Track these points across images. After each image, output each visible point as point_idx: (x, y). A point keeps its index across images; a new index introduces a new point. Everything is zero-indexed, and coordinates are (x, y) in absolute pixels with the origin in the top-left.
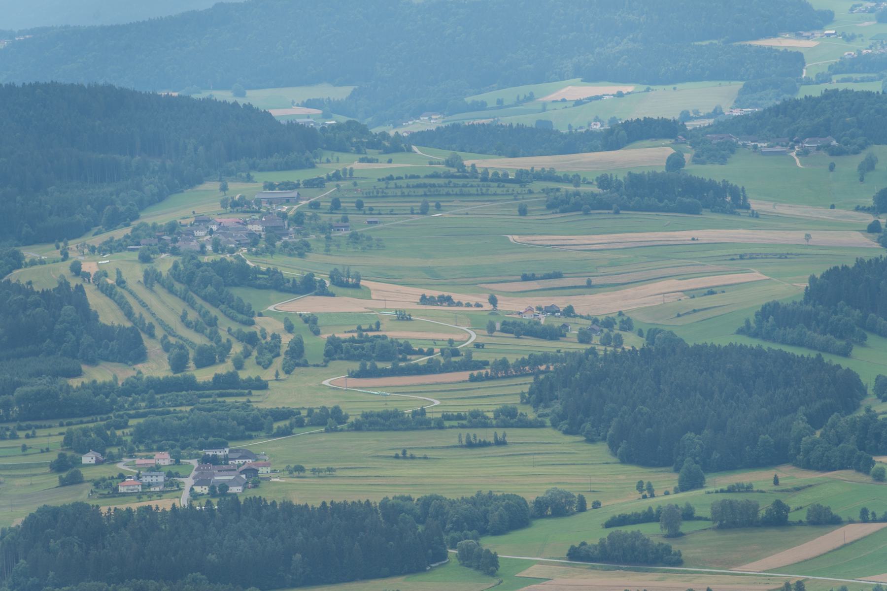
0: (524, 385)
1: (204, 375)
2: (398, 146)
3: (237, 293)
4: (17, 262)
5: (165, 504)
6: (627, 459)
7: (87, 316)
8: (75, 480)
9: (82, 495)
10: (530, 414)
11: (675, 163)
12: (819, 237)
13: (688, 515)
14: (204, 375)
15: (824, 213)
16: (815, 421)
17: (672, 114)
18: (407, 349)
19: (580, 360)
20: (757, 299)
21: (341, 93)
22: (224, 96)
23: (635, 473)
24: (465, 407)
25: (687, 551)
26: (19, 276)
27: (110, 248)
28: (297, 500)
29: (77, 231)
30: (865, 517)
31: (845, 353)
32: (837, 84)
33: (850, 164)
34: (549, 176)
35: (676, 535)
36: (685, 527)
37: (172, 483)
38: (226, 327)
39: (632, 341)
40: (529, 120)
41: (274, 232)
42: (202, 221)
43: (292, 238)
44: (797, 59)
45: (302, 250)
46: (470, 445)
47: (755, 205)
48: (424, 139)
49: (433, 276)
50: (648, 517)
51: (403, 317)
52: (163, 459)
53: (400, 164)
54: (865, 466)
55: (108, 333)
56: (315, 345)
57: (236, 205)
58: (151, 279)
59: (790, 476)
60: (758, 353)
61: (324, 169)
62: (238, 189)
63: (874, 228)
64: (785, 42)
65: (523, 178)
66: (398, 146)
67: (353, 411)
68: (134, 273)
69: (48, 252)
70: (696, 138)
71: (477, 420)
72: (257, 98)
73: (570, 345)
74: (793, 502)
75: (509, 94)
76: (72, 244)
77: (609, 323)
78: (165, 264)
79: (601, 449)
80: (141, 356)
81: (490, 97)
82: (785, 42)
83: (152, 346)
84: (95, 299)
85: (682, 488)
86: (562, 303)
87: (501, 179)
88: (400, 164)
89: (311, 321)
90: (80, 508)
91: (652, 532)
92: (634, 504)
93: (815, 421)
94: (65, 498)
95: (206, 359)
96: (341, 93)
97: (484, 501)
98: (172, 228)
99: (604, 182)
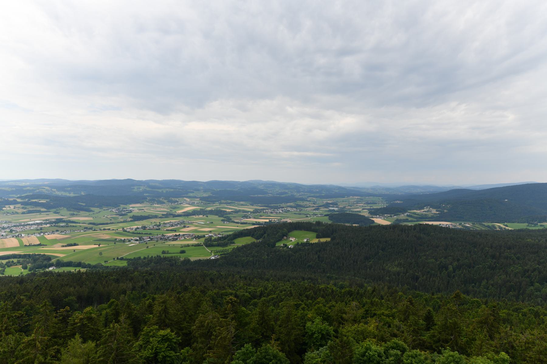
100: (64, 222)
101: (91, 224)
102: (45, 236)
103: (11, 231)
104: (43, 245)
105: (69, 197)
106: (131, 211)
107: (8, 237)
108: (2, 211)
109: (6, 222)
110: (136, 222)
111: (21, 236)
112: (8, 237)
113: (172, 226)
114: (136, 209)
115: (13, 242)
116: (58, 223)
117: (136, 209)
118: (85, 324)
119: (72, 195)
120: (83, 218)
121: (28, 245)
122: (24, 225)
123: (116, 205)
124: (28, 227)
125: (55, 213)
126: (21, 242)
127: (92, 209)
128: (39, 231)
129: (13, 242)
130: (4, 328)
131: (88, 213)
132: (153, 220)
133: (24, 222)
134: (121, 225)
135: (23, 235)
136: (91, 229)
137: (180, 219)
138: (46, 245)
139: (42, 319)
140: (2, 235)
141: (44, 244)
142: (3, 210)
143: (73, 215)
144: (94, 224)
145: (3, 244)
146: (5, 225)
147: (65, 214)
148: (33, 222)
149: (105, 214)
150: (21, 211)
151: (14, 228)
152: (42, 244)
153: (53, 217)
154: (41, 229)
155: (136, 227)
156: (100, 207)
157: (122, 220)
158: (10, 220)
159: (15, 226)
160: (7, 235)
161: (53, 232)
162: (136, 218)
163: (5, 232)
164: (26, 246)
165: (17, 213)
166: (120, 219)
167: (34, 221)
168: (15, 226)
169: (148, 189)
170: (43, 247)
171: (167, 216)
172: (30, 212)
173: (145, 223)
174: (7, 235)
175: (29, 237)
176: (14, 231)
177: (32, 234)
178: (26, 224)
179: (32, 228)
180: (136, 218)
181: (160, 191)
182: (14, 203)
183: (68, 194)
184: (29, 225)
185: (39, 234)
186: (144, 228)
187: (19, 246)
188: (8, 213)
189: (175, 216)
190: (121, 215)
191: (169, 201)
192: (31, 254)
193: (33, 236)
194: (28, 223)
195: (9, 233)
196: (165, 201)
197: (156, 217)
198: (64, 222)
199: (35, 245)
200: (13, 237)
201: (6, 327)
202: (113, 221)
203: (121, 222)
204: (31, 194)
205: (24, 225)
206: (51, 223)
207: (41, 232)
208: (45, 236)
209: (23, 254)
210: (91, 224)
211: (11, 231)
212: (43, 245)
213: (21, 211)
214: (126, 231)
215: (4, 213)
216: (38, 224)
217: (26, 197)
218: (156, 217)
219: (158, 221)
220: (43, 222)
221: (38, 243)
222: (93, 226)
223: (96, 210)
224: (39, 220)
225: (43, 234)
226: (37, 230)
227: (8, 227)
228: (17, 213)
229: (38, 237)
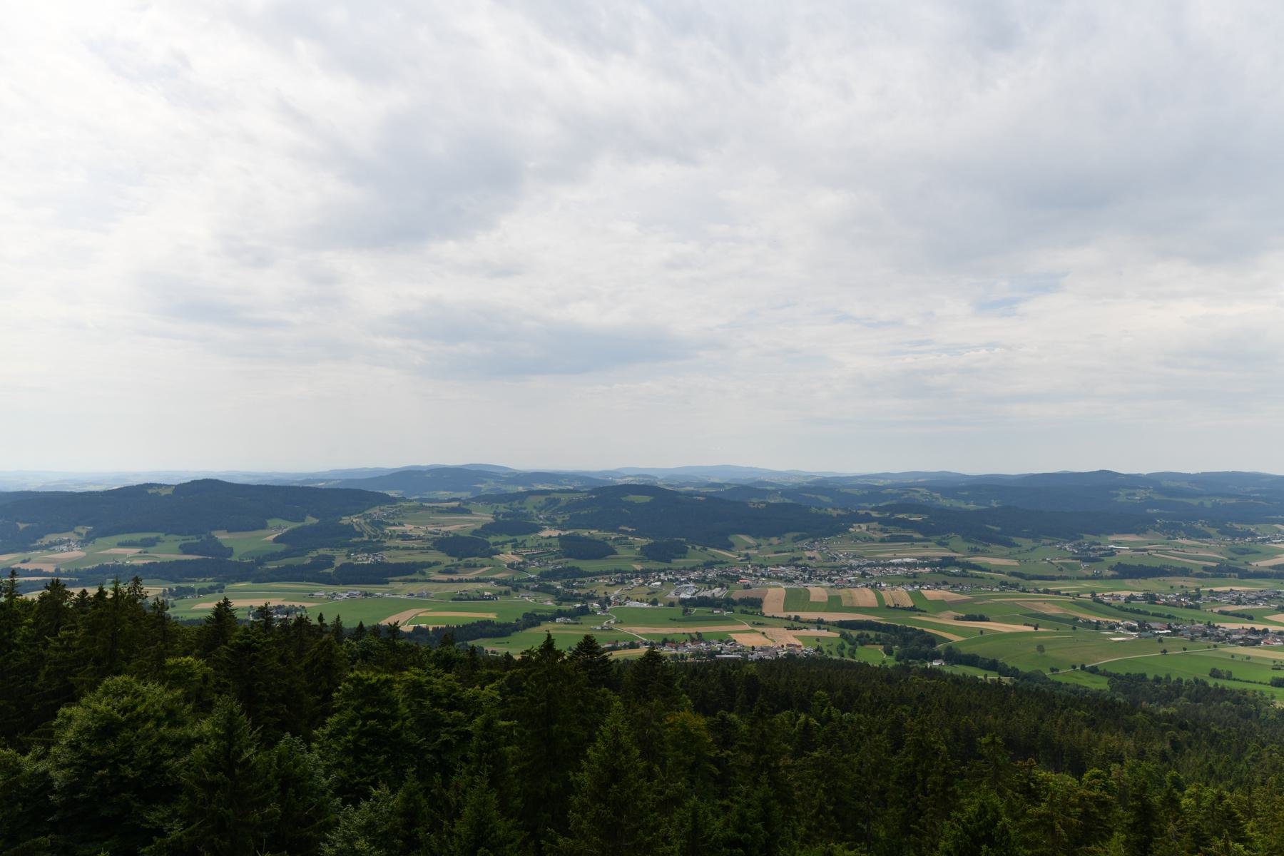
0: (431, 543)
1: (374, 540)
2: (411, 501)
3: (383, 526)
4: (341, 519)
5: (366, 562)
6: (449, 556)
7: (354, 529)
8: (350, 558)
9: (351, 561)
10: (432, 547)
11: (459, 505)
12: (484, 518)
13: (459, 565)
14: (374, 540)
15: (485, 515)
16: (482, 549)
17: (459, 497)
18: (411, 536)
19: (441, 538)
20: (474, 528)
21: (401, 492)
22: (381, 491)
23: (449, 558)
24: (422, 546)
25: (458, 571)
26: (341, 522)
27: (359, 517)
28: (390, 562)
29: (353, 515)
30: (490, 566)
31: (487, 538)
32: (488, 493)
33: (489, 506)
34: (437, 507)
35: (457, 568)
36: (459, 567)
37: (367, 559)
38: (379, 532)
39: (451, 535)
40: (434, 497)
41: (388, 515)
42: (375, 513)
43: (391, 516)
44: (480, 489)
45: (393, 519)
46: (422, 553)
47: (473, 513)
48: (415, 500)
49: (416, 524)
50: (452, 565)
51: (411, 530)
52: (366, 555)
53: (411, 504)
54: (490, 557)
55: (357, 532)
56: (395, 535)
57: (383, 511)
58: (366, 523)
59: (477, 559)
60: (473, 538)
61: (398, 505)
62: (382, 508)
63: (493, 517)
64: (478, 486)
65: (433, 507)
66: (411, 501)
67: (401, 547)
68: (363, 522)
69: (348, 518)
70: (464, 501)
71: (423, 548)
72: (386, 492)
73: (440, 536)
74: (477, 563)
75: (431, 493)
76: (352, 517)
77: (447, 532)
78: (368, 520)
79: (444, 554)
80: (363, 536)
81: (427, 493)
82: (478, 486)
83: (365, 535)
84: (355, 526)
85: (459, 560)
86: (439, 528)
87: (429, 507)
88: (411, 504)
89: (394, 531)
90: (350, 563)
91: (453, 568)
92: (449, 563)
93: (482, 549)
94: (347, 561)
95: (375, 537)
96: (401, 492)
97: (424, 562)
98: (370, 514)
99: (447, 508)
100: (957, 564)
101: (1013, 574)
102: (921, 591)
103: (864, 574)
104: (919, 610)
105: (967, 512)
106: (1112, 553)
107: (858, 586)
108: (848, 535)
109: (854, 557)
110: (1128, 582)
111: (880, 586)
112: (858, 586)
113: (1239, 602)
114: (1124, 546)
115: (866, 597)
116: (946, 566)
117: (1124, 546)
118: (1094, 813)
119: (972, 506)
120: (995, 560)
121: (893, 606)
122: (884, 566)
123: (1071, 535)
124: (891, 570)
125: (940, 544)
126: (880, 598)
127: (1016, 540)
128: (912, 581)
129: (866, 597)
130: (941, 769)
131: (1006, 550)
132: (1178, 581)
133: (884, 559)
134: (1087, 584)
135: (883, 585)
136: (1015, 586)
137: (1268, 586)
138: (925, 612)
139: (989, 772)
140: (850, 581)
141: (924, 609)
142: (850, 533)
143: (975, 551)
144: (1021, 576)
145: (852, 598)
146: (854, 562)
147: (958, 549)
148: (900, 560)
149: (1049, 555)
150: (878, 535)
151: (867, 570)
152: (917, 608)
153: (936, 553)
154: (915, 576)
155: (1128, 593)
156: (1035, 535)
157: (1089, 573)
158: (860, 551)
159: (868, 565)
160: (857, 582)
161: (937, 586)
162: (1127, 572)
163: (854, 575)
164: (888, 607)
165: (872, 540)
166: (1085, 569)
167: (902, 558)
168: (868, 565)
169: (1157, 497)
170: (919, 615)
171: (1220, 572)
172: (894, 539)
173: (1152, 585)
174: (857, 582)
175: (893, 589)
176: (868, 574)
177: (899, 586)
178: (888, 562)
179: (898, 573)
180: (1127, 572)
181: (1196, 502)
182: (867, 519)
183: (962, 505)
184: (893, 565)
185: (913, 586)
186: (1151, 599)
187: (877, 605)
188: (858, 539)
189: (1245, 575)
190: (1085, 560)
191: (1222, 533)
192: (899, 625)
193: (900, 589)
194: (890, 561)
195: (861, 579)
196: (1213, 531)
197: (1185, 572)
198: (957, 564)
199: (904, 609)
200: (867, 586)
201: (945, 768)
202: (1066, 573)
203: (1087, 578)
204: (894, 502)
205: (884, 566)
206: (931, 565)
207: (916, 583)
208: (922, 591)
209: (885, 623)
210: (1013, 574)
211: (864, 574)
212: (919, 610)
213: (878, 535)
214: (1100, 601)
215: (851, 539)
216: (908, 565)
217: (888, 508)
218: (1185, 572)
219: (1191, 584)
220: (918, 562)
221: (910, 604)
222: (1019, 580)
223: (1026, 543)
224: (910, 558)
225: (918, 587)
226: (908, 577)
227: (859, 566)
228: (872, 540)
229: (909, 592)
